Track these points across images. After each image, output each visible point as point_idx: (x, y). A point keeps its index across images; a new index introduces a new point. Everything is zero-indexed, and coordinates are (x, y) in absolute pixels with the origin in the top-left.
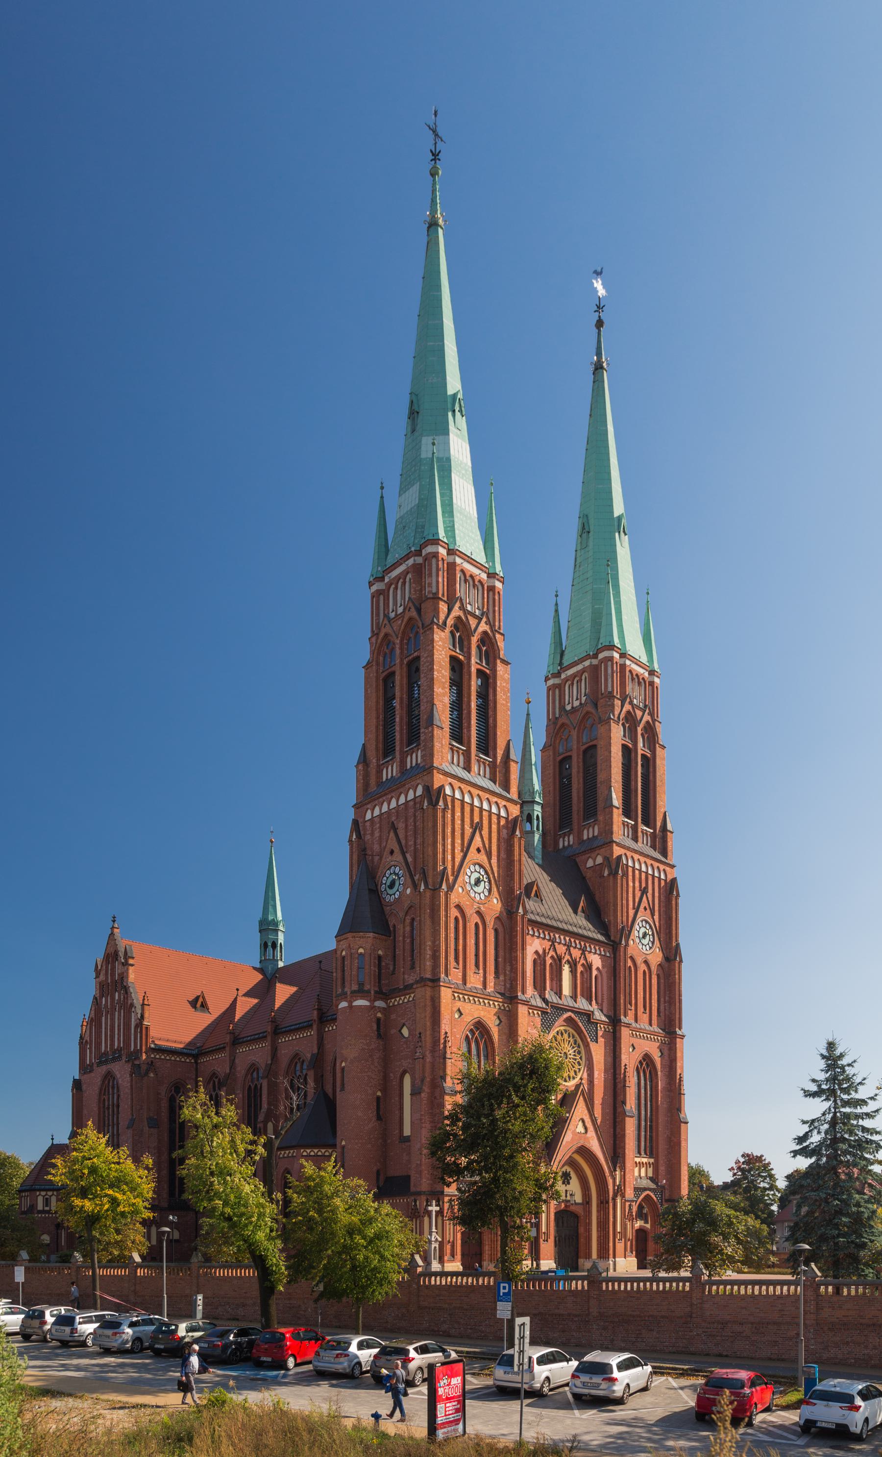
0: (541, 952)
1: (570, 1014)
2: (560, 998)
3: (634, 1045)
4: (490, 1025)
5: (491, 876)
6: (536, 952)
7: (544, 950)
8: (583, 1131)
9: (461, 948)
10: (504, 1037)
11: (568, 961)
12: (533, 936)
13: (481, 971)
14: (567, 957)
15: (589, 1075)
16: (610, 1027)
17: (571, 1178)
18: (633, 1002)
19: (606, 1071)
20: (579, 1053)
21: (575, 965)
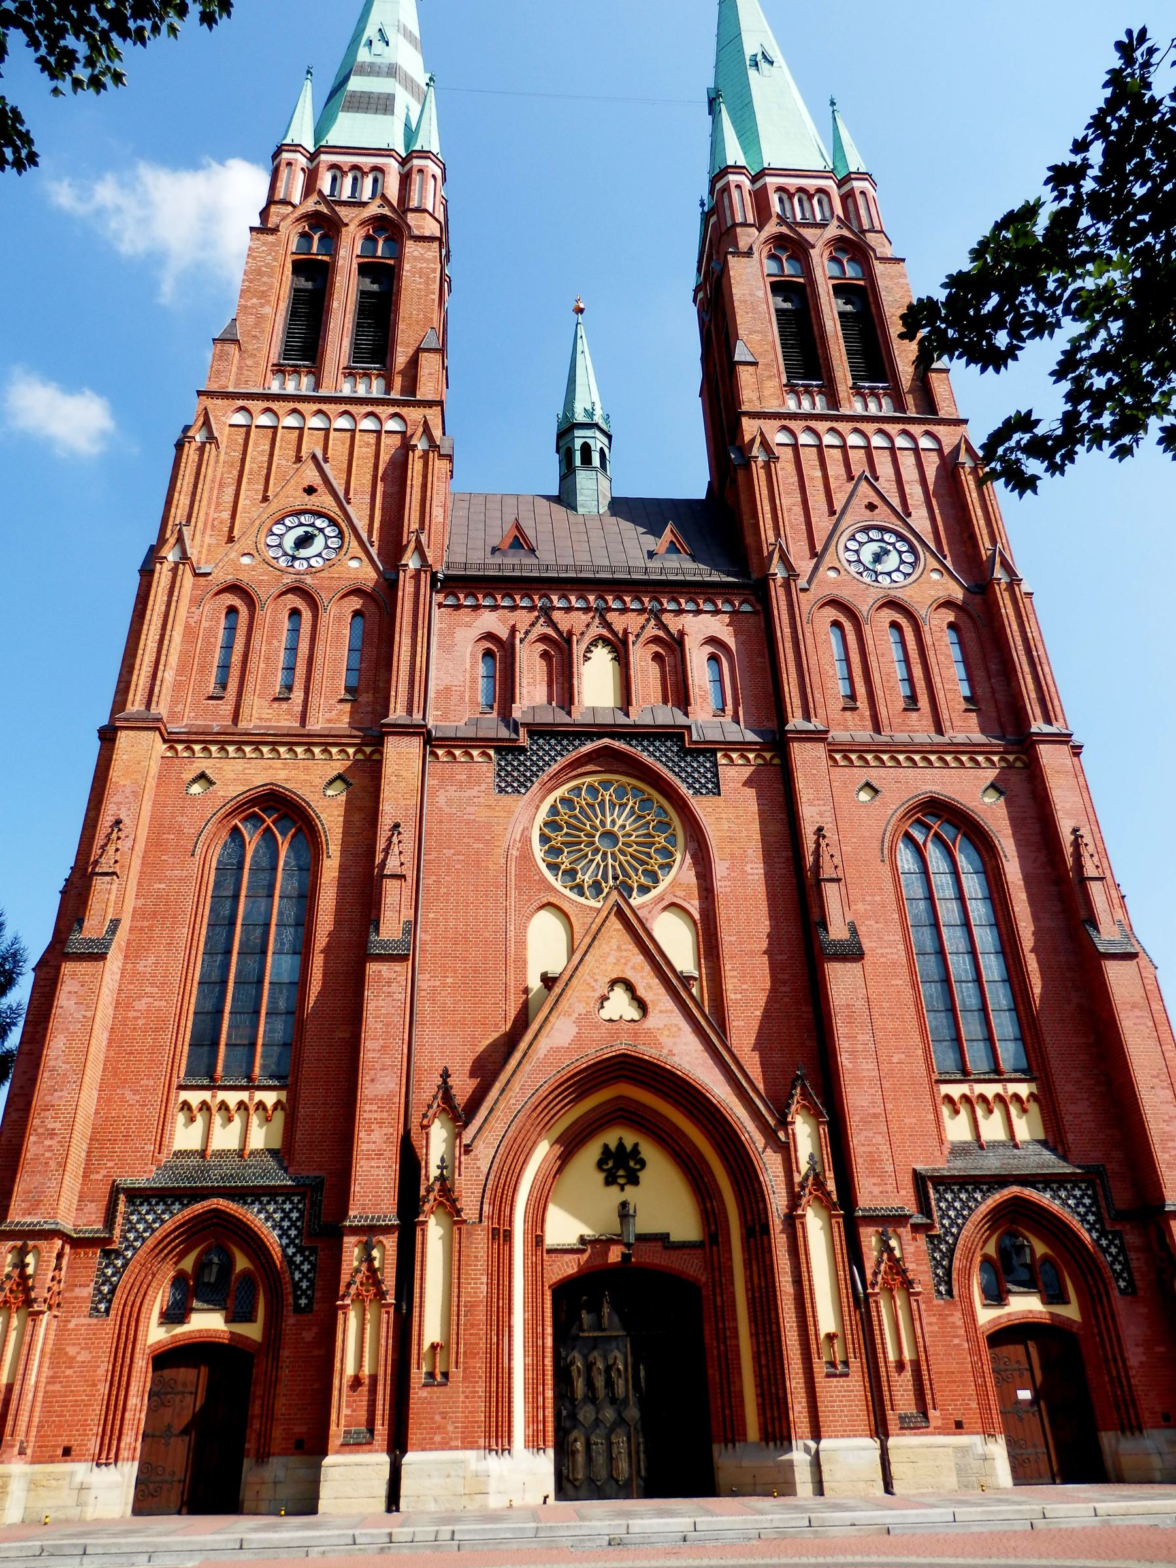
0: (504, 634)
1: (606, 741)
2: (569, 714)
3: (874, 783)
4: (309, 797)
5: (343, 525)
6: (490, 636)
7: (513, 630)
8: (633, 1013)
9: (236, 659)
10: (356, 817)
11: (606, 642)
12: (476, 608)
13: (297, 695)
14: (596, 630)
15: (698, 876)
16: (768, 755)
17: (643, 1164)
18: (861, 690)
19: (768, 857)
20: (664, 826)
21: (625, 642)
